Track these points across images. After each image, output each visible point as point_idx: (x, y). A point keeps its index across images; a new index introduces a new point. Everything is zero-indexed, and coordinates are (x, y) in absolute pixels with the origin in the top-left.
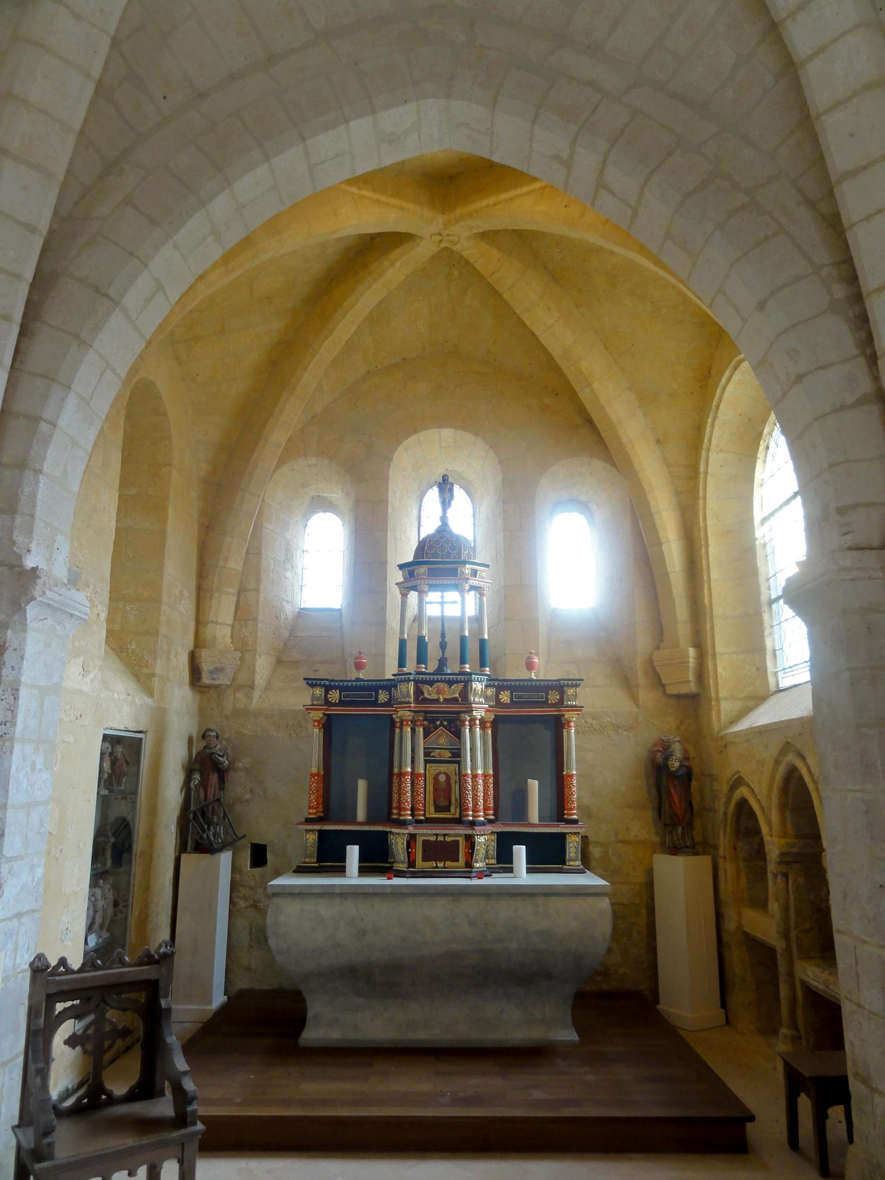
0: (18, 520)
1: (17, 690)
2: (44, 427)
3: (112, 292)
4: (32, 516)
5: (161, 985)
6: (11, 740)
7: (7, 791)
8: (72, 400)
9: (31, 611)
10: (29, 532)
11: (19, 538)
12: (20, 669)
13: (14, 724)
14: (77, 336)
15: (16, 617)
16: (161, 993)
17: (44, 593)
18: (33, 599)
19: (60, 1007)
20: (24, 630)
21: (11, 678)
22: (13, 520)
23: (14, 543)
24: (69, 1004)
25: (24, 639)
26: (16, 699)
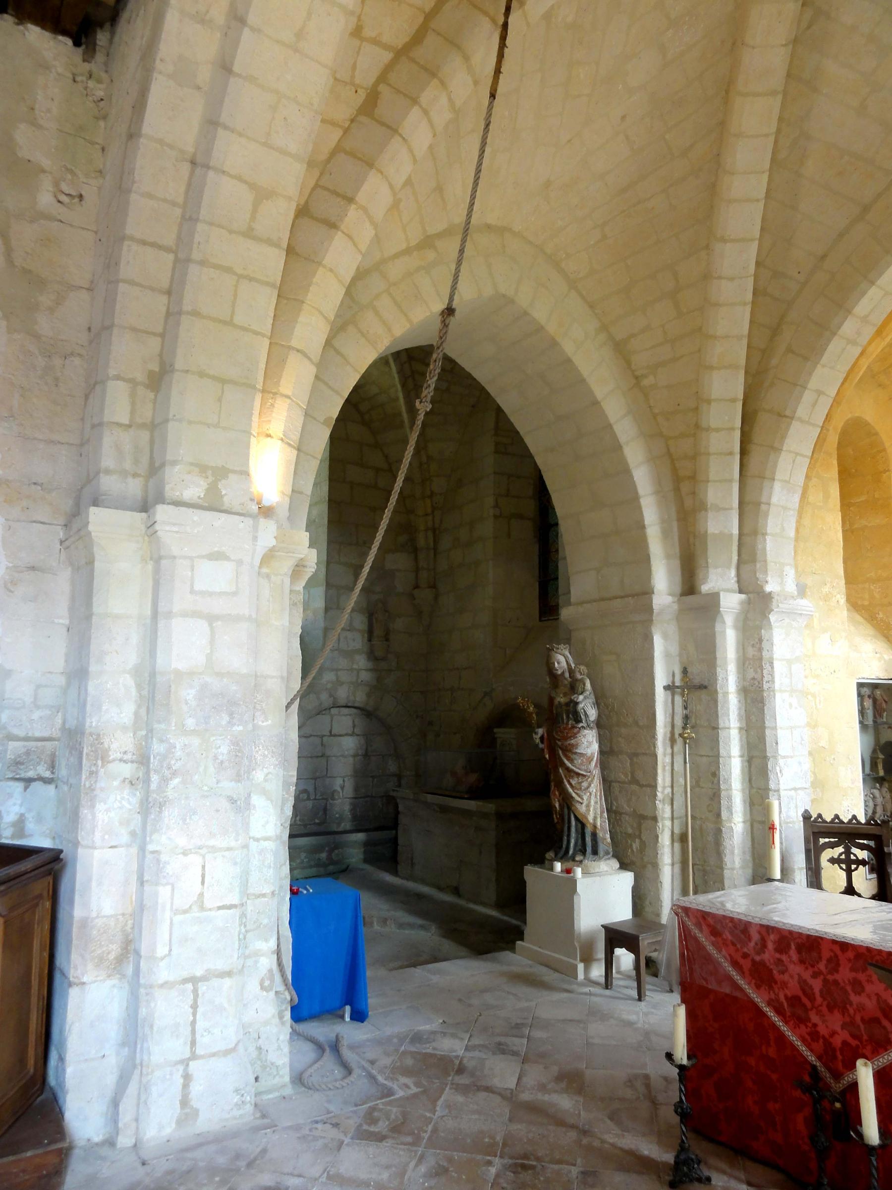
0: (758, 565)
1: (772, 663)
2: (763, 507)
3: (788, 413)
4: (765, 561)
5: (883, 838)
6: (774, 691)
7: (776, 719)
8: (777, 486)
9: (772, 617)
10: (766, 572)
11: (760, 575)
12: (772, 651)
13: (773, 682)
14: (772, 448)
15: (764, 622)
16: (885, 843)
17: (778, 605)
18: (773, 610)
19: (822, 841)
20: (771, 629)
21: (768, 656)
22: (755, 566)
23: (757, 579)
24: (827, 840)
25: (772, 634)
26: (772, 668)
